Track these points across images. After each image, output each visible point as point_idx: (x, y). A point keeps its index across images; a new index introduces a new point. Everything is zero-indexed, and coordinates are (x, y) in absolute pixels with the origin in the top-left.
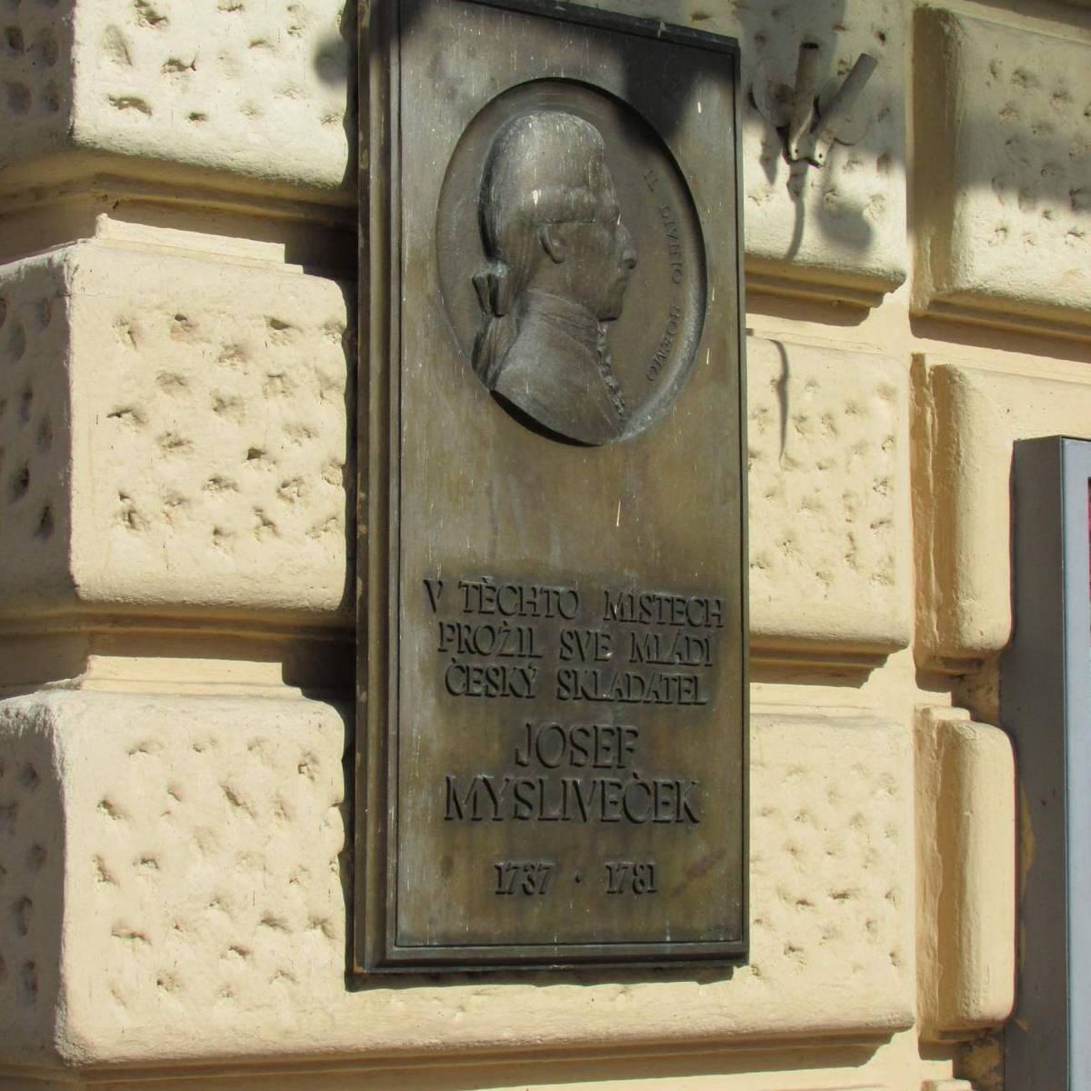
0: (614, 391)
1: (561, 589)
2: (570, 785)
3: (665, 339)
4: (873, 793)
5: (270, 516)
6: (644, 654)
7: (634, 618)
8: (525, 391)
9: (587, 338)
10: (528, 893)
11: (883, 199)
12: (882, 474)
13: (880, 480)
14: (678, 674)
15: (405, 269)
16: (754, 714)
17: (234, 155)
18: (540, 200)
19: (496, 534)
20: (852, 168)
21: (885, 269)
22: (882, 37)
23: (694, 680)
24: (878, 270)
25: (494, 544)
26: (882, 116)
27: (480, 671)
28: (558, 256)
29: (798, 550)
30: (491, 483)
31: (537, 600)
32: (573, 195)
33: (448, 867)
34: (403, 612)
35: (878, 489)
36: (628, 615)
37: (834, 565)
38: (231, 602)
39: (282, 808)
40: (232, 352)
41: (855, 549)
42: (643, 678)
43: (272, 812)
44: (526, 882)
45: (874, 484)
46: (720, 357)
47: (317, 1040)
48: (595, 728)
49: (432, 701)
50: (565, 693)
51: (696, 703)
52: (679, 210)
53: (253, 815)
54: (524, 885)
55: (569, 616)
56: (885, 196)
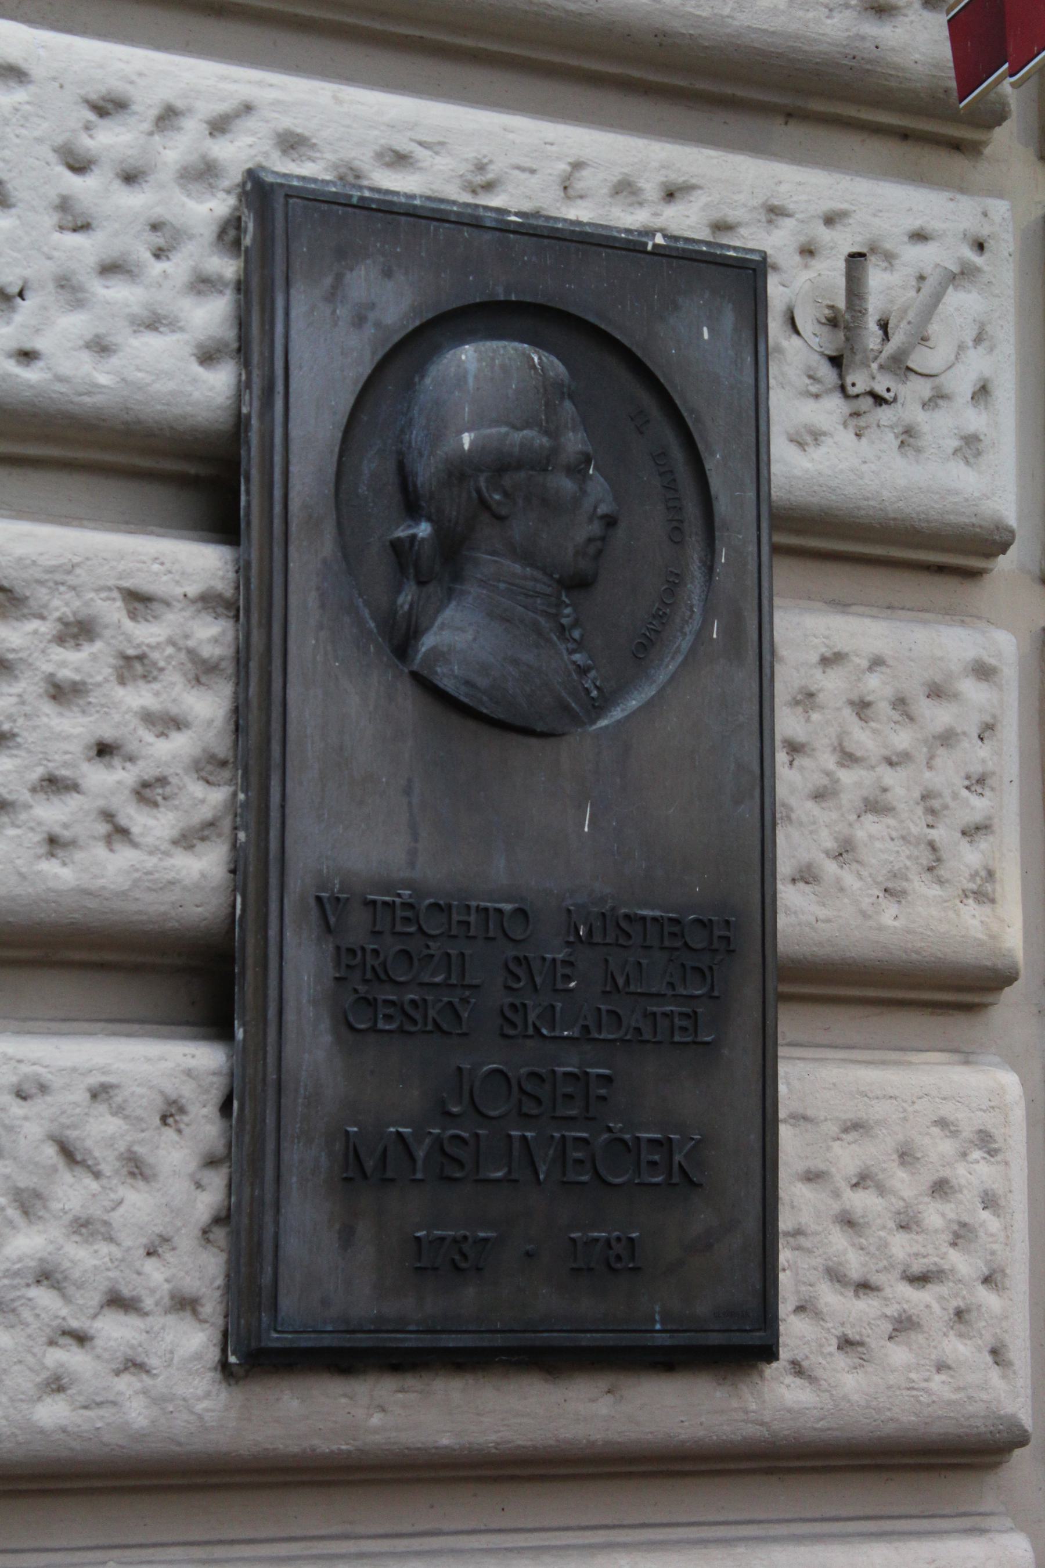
0: (583, 671)
1: (507, 907)
2: (516, 1145)
3: (659, 609)
4: (964, 1155)
5: (123, 821)
6: (621, 981)
7: (608, 940)
8: (452, 670)
9: (544, 608)
10: (457, 1269)
11: (980, 440)
12: (976, 769)
13: (975, 777)
14: (669, 1008)
15: (293, 528)
16: (784, 1058)
17: (77, 399)
18: (472, 443)
19: (416, 840)
20: (937, 405)
21: (983, 523)
22: (980, 247)
23: (693, 1016)
24: (973, 525)
25: (413, 853)
26: (978, 340)
27: (392, 1003)
28: (504, 512)
29: (857, 862)
30: (410, 780)
31: (472, 918)
32: (517, 436)
33: (347, 1237)
34: (288, 934)
35: (973, 789)
36: (597, 938)
37: (907, 880)
38: (72, 923)
39: (137, 1167)
40: (75, 630)
41: (939, 860)
42: (619, 1011)
43: (124, 1171)
44: (457, 1257)
45: (967, 783)
46: (734, 632)
47: (180, 1444)
48: (554, 1072)
49: (327, 1039)
50: (511, 1032)
51: (695, 1043)
52: (678, 455)
53: (97, 1175)
54: (453, 1260)
55: (519, 937)
56: (982, 437)
